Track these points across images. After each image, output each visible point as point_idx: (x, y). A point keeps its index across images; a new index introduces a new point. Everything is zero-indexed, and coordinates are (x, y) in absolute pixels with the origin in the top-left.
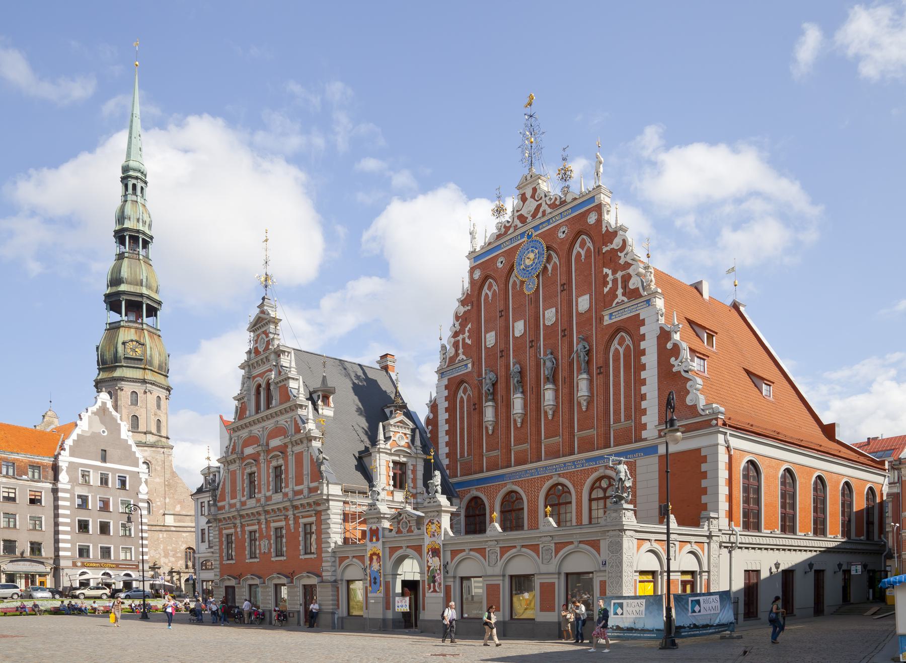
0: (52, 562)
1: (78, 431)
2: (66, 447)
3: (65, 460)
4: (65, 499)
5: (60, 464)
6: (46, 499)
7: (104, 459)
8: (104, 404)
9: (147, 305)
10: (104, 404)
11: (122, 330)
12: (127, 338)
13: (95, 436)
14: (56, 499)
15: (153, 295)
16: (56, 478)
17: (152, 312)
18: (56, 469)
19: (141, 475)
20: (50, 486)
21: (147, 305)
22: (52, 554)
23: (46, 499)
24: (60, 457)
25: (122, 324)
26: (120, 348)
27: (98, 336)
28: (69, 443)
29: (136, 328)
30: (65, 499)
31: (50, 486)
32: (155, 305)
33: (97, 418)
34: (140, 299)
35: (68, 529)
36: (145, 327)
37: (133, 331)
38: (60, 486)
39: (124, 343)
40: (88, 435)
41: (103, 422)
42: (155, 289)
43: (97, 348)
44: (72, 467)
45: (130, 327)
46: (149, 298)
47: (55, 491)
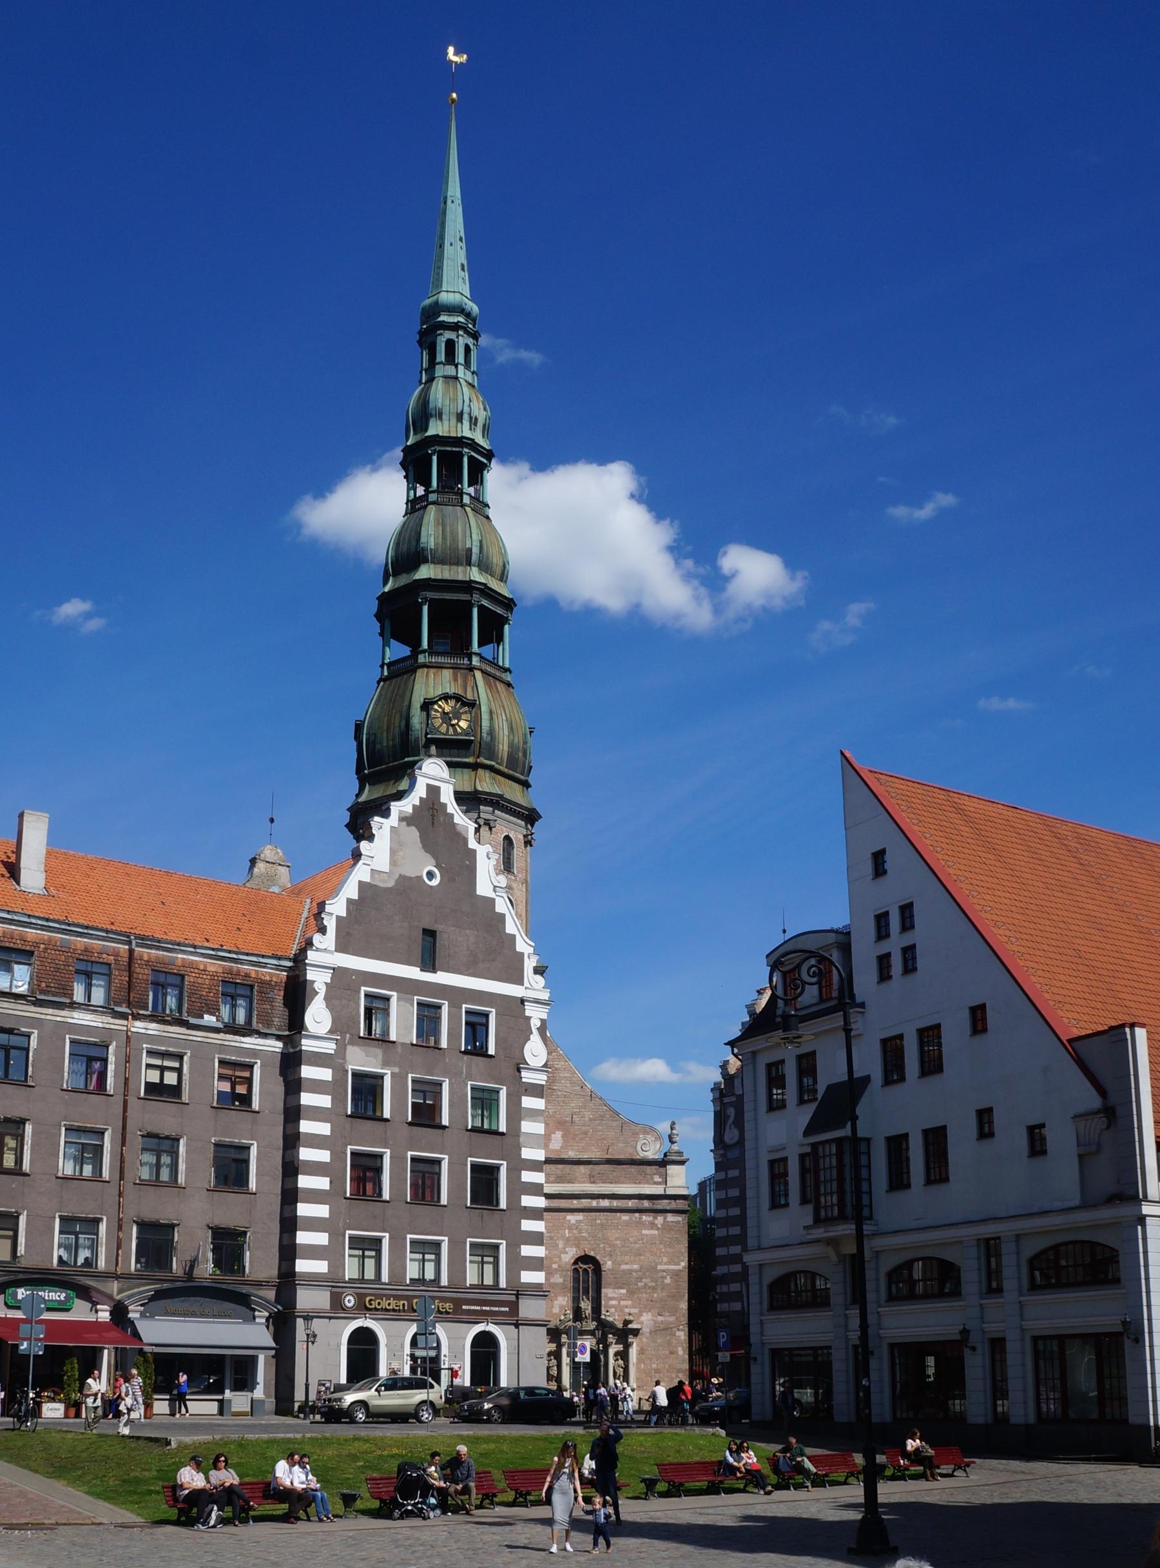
0: (271, 1294)
1: (361, 873)
2: (330, 923)
3: (325, 958)
4: (318, 1087)
5: (310, 975)
6: (263, 1088)
7: (429, 963)
8: (433, 791)
9: (482, 609)
10: (433, 791)
11: (421, 674)
12: (432, 693)
13: (408, 887)
14: (293, 1086)
15: (494, 585)
16: (296, 1023)
17: (492, 631)
18: (296, 993)
19: (530, 1010)
20: (276, 1046)
21: (482, 609)
22: (270, 1270)
23: (263, 1088)
24: (312, 956)
25: (421, 659)
26: (417, 719)
27: (361, 697)
28: (337, 908)
29: (455, 668)
30: (318, 1087)
31: (276, 1046)
32: (499, 611)
33: (413, 833)
34: (464, 597)
35: (322, 1183)
36: (475, 661)
37: (447, 674)
38: (307, 1045)
39: (427, 706)
40: (391, 884)
41: (429, 845)
42: (498, 571)
43: (359, 727)
44: (342, 980)
45: (440, 667)
46: (486, 592)
47: (291, 1061)
